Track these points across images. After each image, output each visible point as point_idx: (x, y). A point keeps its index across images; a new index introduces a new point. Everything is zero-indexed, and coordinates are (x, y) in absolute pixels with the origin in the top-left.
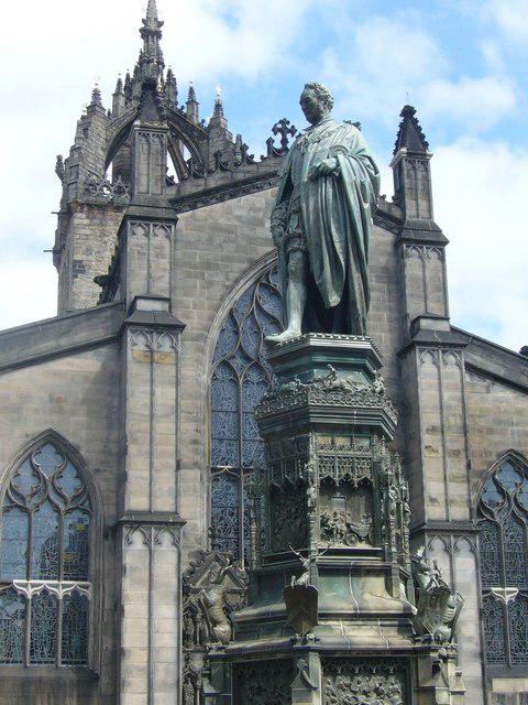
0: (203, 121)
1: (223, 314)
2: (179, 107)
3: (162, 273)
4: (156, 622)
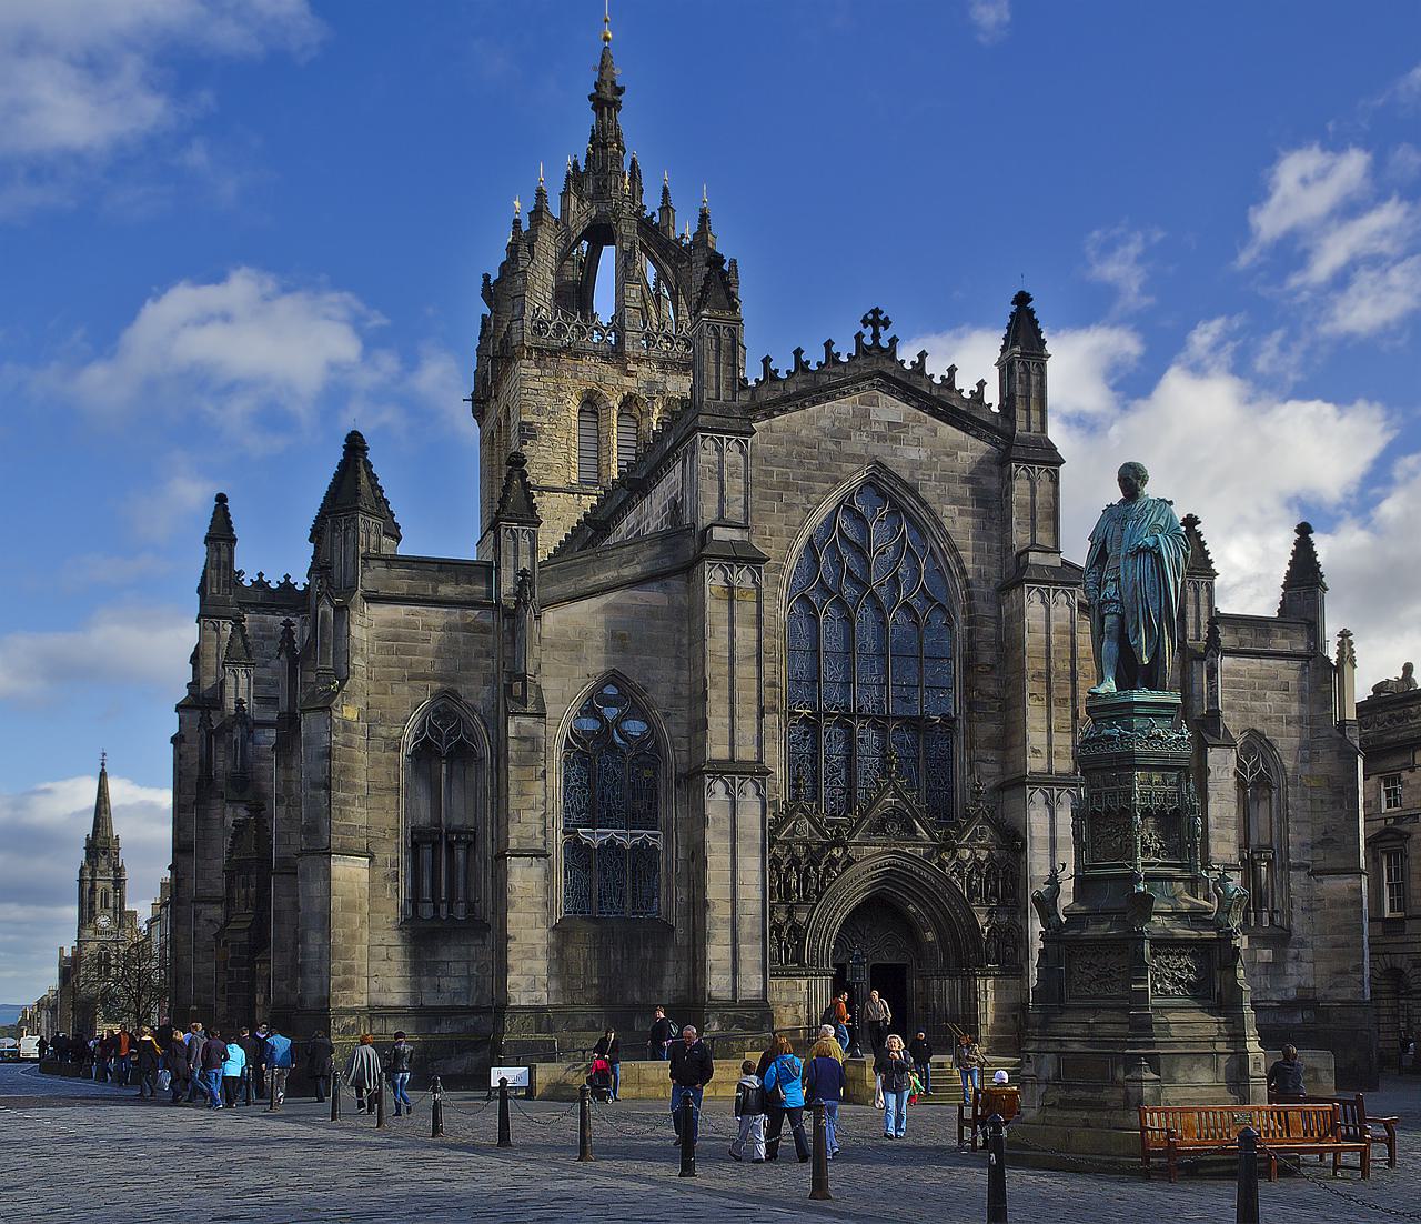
0: (683, 236)
1: (802, 541)
2: (647, 213)
3: (738, 496)
4: (740, 874)
